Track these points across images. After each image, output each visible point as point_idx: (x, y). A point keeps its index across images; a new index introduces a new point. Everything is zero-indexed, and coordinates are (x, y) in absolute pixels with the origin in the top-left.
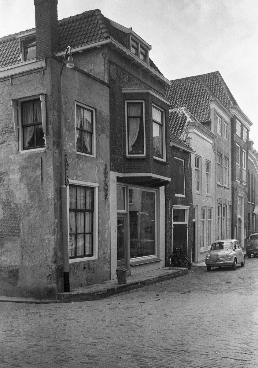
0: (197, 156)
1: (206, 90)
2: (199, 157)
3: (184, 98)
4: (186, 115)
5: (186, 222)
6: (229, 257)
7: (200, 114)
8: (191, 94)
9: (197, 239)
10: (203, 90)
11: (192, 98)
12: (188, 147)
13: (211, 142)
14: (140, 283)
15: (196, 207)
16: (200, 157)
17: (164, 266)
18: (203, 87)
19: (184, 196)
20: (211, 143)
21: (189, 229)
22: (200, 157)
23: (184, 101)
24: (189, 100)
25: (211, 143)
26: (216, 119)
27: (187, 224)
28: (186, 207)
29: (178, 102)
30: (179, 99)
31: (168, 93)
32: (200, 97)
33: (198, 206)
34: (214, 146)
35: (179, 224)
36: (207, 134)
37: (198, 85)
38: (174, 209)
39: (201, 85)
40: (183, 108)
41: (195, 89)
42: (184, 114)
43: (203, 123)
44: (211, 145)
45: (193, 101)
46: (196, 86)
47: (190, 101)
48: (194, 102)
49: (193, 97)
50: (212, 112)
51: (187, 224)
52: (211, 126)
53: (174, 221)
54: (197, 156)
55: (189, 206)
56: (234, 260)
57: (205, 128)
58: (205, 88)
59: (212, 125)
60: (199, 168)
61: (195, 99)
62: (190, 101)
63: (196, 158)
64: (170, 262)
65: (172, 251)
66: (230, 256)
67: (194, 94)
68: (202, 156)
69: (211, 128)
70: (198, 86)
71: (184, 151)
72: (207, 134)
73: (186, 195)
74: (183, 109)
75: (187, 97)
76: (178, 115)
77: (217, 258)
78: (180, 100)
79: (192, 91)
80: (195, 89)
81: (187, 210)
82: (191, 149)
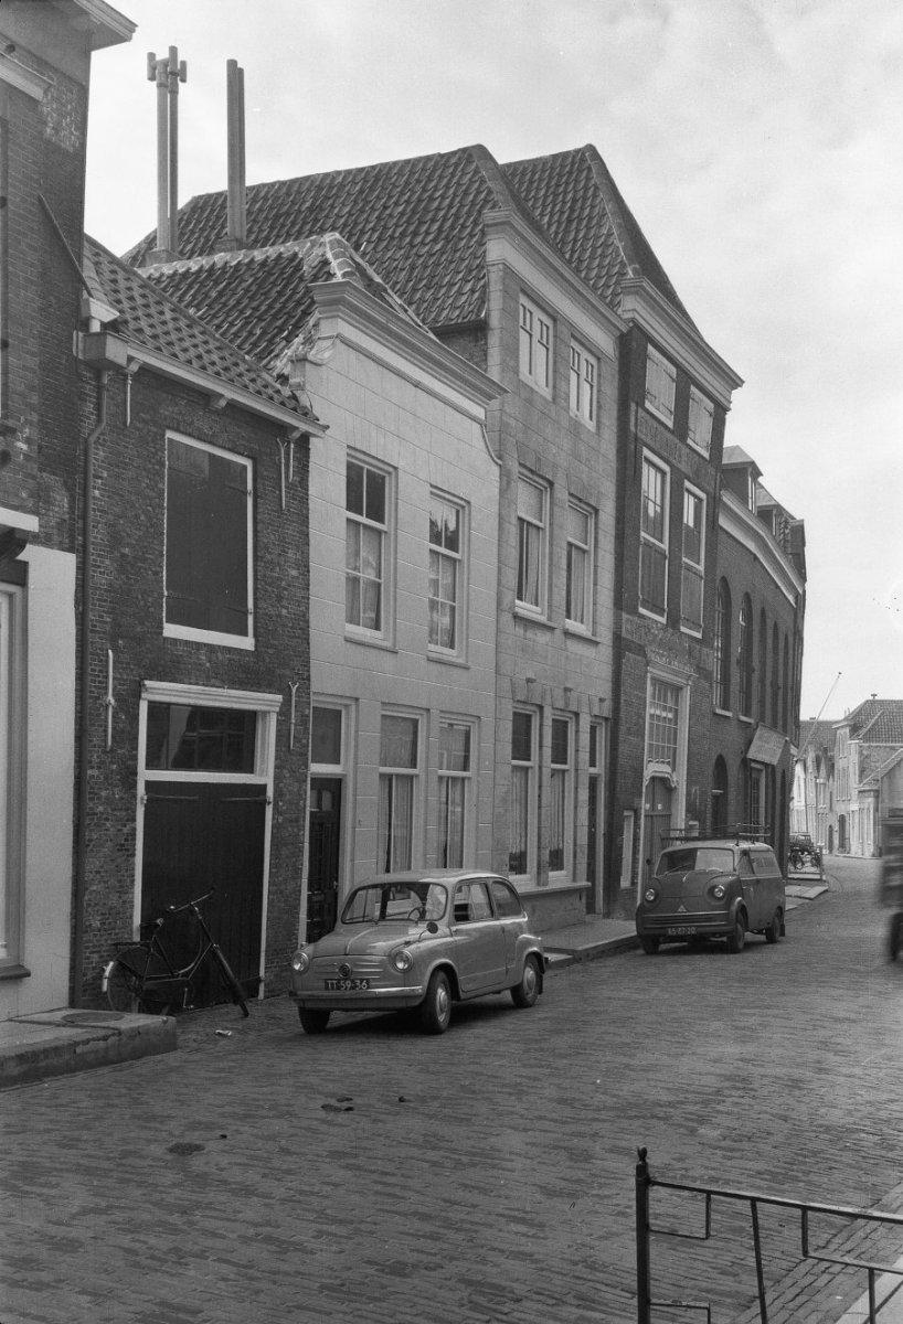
0: (353, 453)
1: (490, 192)
2: (386, 468)
3: (397, 225)
4: (334, 264)
5: (264, 774)
6: (400, 965)
7: (449, 290)
8: (426, 210)
9: (353, 860)
10: (479, 192)
11: (426, 225)
12: (294, 404)
13: (479, 412)
14: (12, 1064)
15: (346, 706)
16: (391, 469)
17: (66, 1004)
18: (483, 181)
19: (247, 643)
20: (474, 419)
21: (276, 810)
22: (391, 469)
23: (392, 238)
24: (415, 234)
25: (474, 419)
26: (510, 313)
27: (265, 786)
28: (264, 702)
29: (369, 242)
30: (374, 230)
31: (332, 207)
32: (461, 221)
33: (357, 699)
34: (500, 443)
35: (242, 782)
36: (453, 373)
37: (464, 174)
38: (153, 706)
39: (476, 171)
40: (328, 237)
41: (447, 187)
42: (326, 263)
43: (446, 333)
44: (476, 427)
45: (431, 237)
46: (453, 175)
47: (419, 239)
48: (435, 241)
49: (433, 221)
50: (495, 276)
51: (265, 786)
52: (486, 344)
53: (149, 766)
54: (353, 453)
55: (279, 698)
56: (426, 984)
57: (451, 355)
58: (489, 184)
59: (494, 340)
60: (381, 519)
61: (440, 230)
62: (419, 239)
63: (350, 466)
64: (105, 982)
65: (137, 920)
66: (406, 960)
67: (438, 209)
68: (400, 464)
69: (486, 355)
70: (461, 177)
71: (232, 405)
72: (453, 373)
73: (255, 636)
74: (327, 240)
75: (408, 222)
76: (298, 267)
77: (343, 969)
78: (376, 235)
79: (431, 199)
80: (447, 187)
81: (265, 713)
82: (306, 414)
